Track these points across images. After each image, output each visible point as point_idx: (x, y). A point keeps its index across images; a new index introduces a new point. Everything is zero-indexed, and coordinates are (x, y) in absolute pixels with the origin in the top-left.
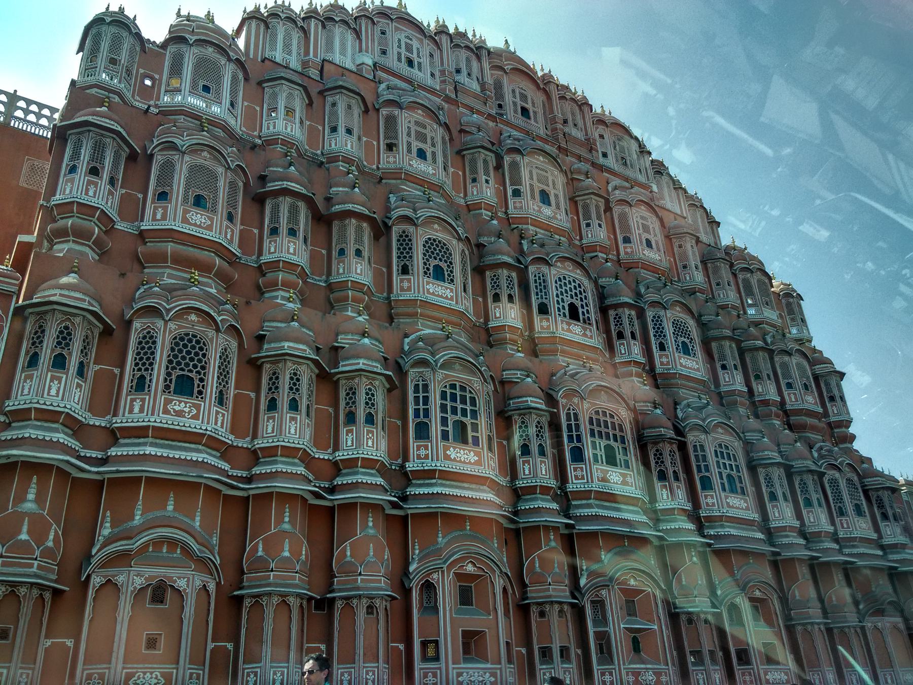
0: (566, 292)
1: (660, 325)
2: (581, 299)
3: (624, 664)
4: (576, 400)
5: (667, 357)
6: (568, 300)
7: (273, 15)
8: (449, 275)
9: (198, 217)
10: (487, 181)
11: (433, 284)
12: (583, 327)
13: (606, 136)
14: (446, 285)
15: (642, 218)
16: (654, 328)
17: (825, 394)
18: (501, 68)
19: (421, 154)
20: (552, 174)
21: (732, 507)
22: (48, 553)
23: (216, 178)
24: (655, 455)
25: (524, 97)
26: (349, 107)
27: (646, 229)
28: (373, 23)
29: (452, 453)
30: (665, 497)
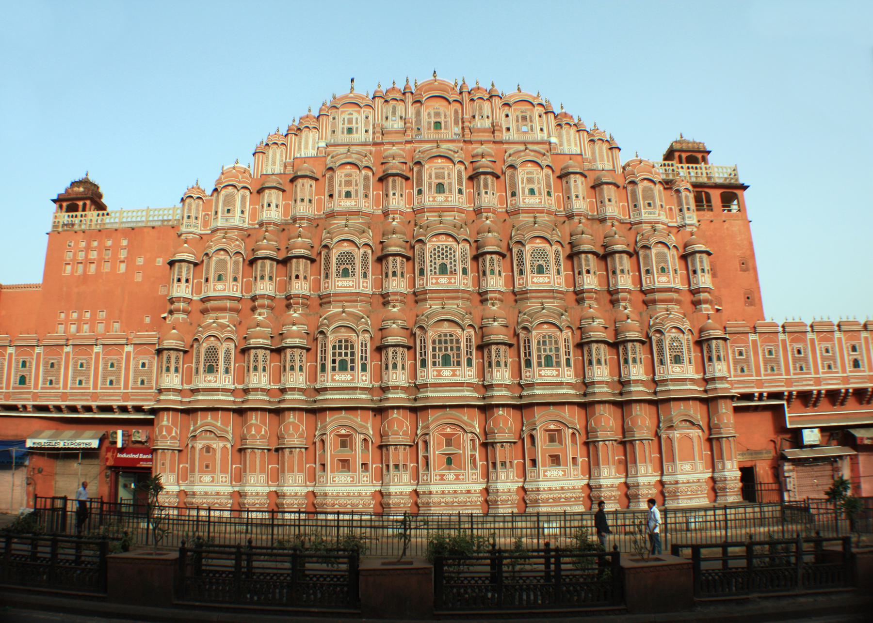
0: (439, 256)
2: (451, 258)
3: (434, 470)
6: (439, 262)
9: (220, 286)
10: (394, 194)
13: (510, 115)
14: (350, 278)
17: (690, 268)
18: (419, 102)
19: (348, 195)
22: (173, 438)
23: (226, 263)
25: (437, 114)
26: (303, 185)
27: (530, 181)
29: (337, 377)
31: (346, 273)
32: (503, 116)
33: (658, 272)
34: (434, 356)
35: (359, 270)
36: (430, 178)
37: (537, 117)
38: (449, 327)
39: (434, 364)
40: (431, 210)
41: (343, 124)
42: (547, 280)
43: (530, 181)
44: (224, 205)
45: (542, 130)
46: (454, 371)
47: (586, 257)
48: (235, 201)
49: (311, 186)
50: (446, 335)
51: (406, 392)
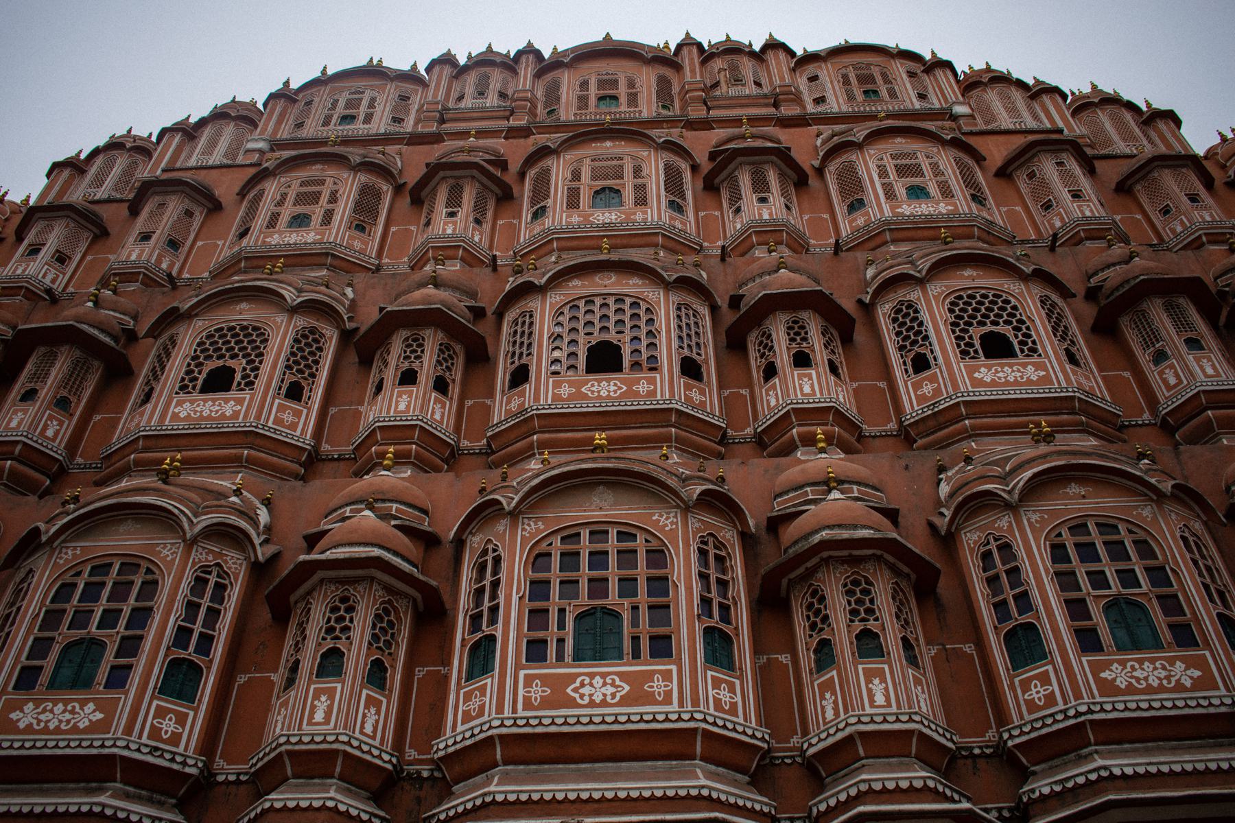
1: (915, 319)
4: (502, 526)
5: (933, 379)
7: (96, 152)
8: (243, 378)
11: (192, 402)
12: (623, 381)
14: (233, 394)
15: (893, 157)
16: (898, 334)
19: (300, 221)
20: (634, 158)
21: (1131, 690)
24: (810, 606)
25: (608, 83)
28: (295, 101)
29: (26, 716)
30: (830, 715)
31: (219, 382)
32: (802, 83)
34: (538, 617)
36: (576, 176)
37: (905, 76)
38: (615, 504)
39: (536, 651)
42: (1031, 373)
45: (922, 97)
47: (1170, 308)
49: (189, 213)
50: (599, 534)
51: (377, 798)
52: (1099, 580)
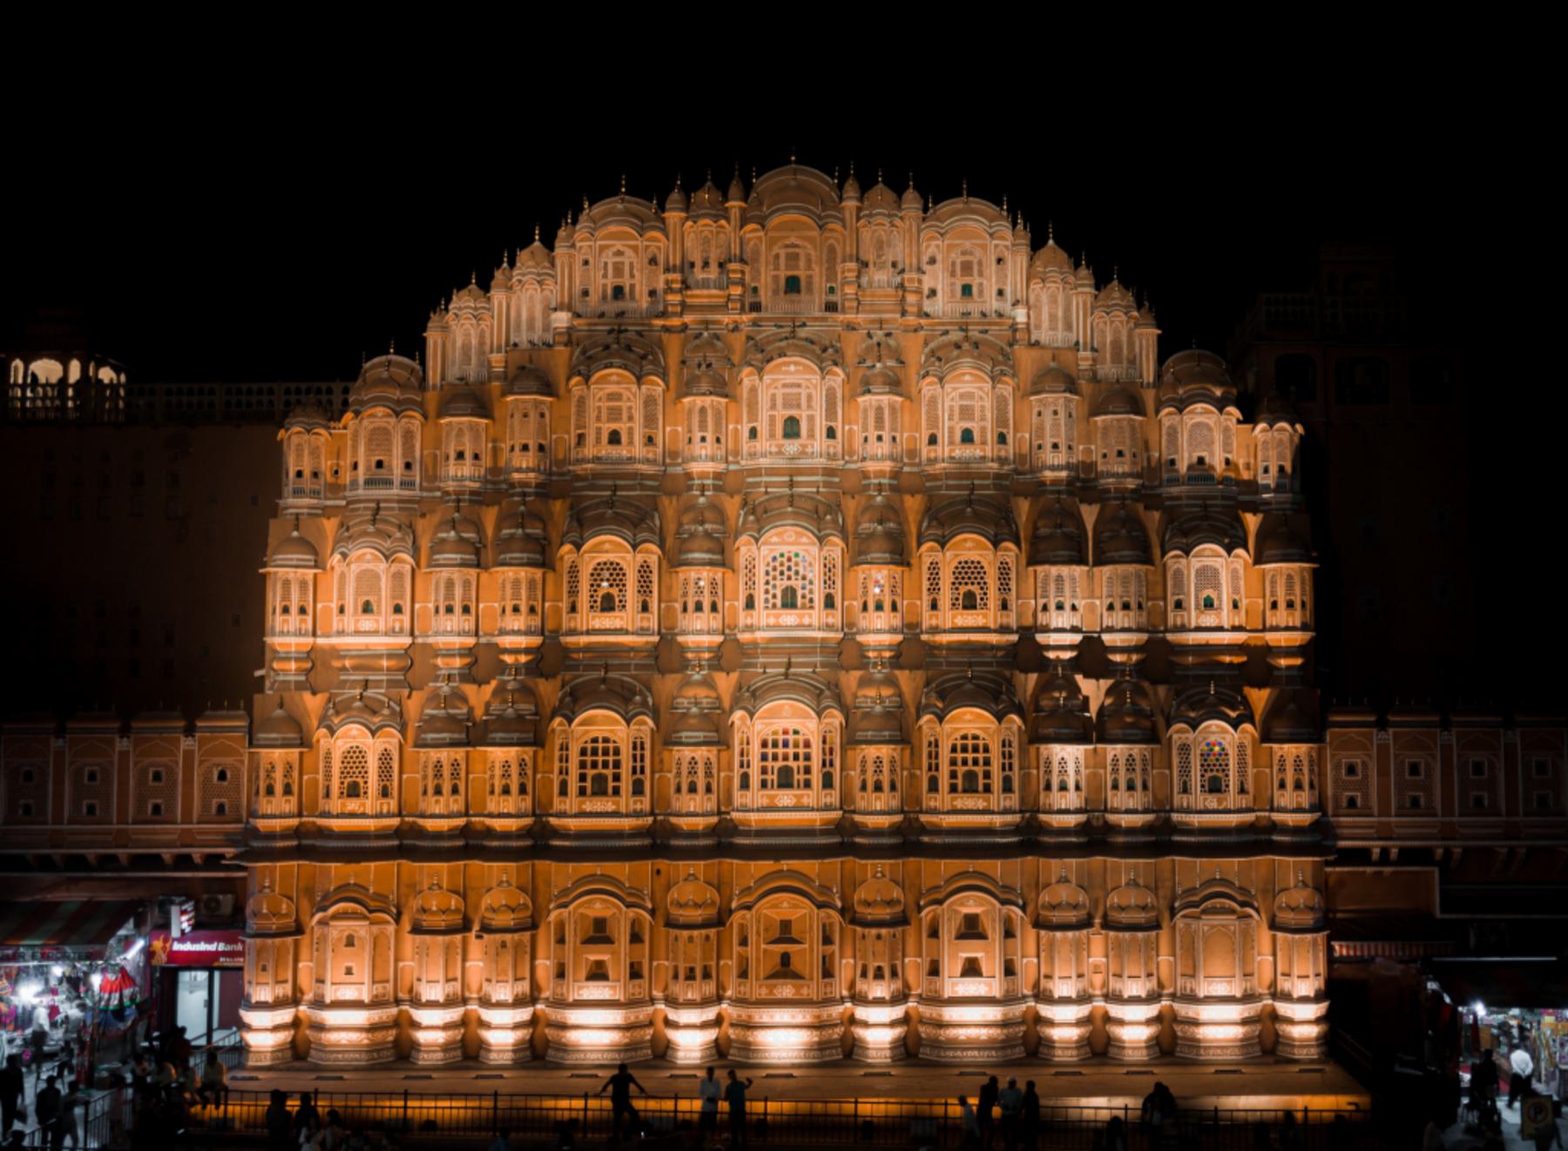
10: (703, 439)
14: (616, 613)
27: (966, 412)
31: (608, 605)
33: (1197, 608)
34: (764, 771)
35: (632, 596)
36: (773, 407)
39: (764, 784)
40: (771, 471)
41: (605, 276)
43: (966, 412)
44: (370, 451)
45: (1000, 293)
46: (799, 797)
48: (391, 444)
50: (785, 732)
52: (965, 762)
